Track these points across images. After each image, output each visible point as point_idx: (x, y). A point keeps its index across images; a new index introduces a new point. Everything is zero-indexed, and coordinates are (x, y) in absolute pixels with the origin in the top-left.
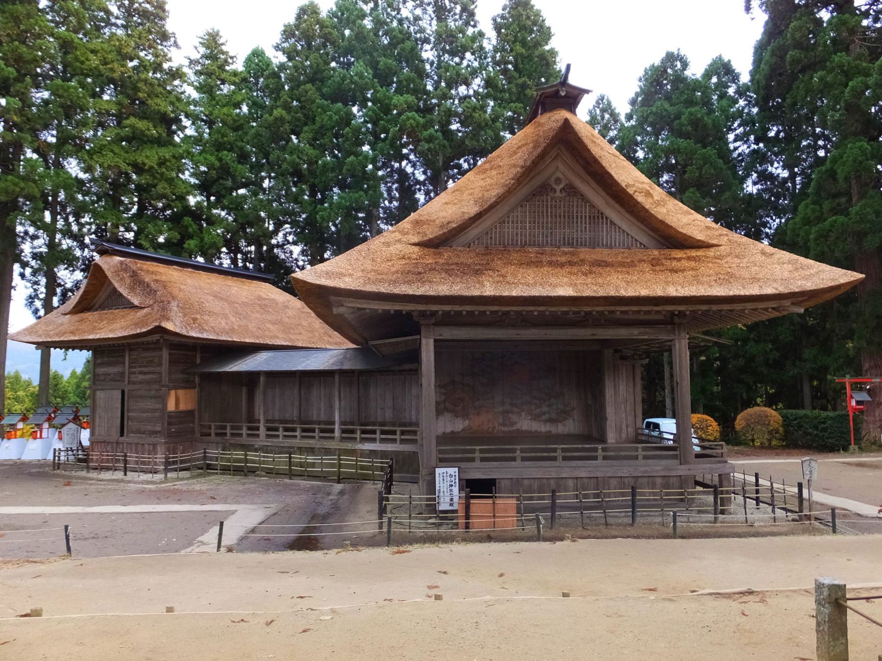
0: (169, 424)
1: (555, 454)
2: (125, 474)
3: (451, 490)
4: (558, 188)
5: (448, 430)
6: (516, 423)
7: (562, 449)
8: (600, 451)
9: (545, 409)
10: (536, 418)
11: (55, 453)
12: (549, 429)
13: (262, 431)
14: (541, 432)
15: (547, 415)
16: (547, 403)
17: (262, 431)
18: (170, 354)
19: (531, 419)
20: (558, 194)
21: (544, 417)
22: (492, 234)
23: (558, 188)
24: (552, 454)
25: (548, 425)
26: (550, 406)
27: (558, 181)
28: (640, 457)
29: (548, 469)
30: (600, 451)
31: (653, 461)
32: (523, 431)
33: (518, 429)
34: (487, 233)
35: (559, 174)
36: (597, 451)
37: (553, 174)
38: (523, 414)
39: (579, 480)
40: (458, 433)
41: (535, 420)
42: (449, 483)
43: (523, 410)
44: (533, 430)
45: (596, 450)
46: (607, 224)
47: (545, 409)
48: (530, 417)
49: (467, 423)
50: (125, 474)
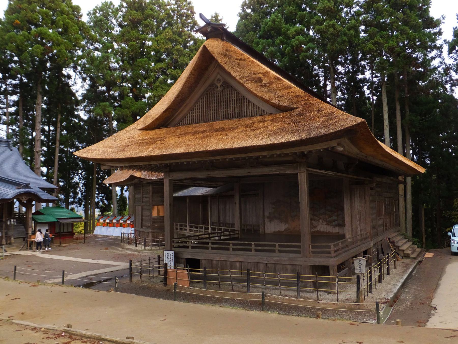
0: (154, 222)
1: (228, 247)
2: (136, 246)
3: (170, 263)
4: (219, 85)
5: (277, 230)
6: (316, 227)
7: (232, 243)
8: (253, 246)
9: (335, 218)
10: (329, 223)
11: (122, 235)
12: (337, 231)
13: (188, 228)
14: (332, 233)
15: (336, 222)
16: (336, 214)
17: (188, 228)
18: (153, 188)
19: (326, 224)
20: (219, 88)
21: (334, 223)
22: (187, 117)
23: (219, 85)
24: (227, 246)
25: (337, 228)
26: (338, 216)
27: (219, 80)
28: (277, 251)
29: (222, 255)
30: (253, 246)
31: (284, 254)
32: (321, 232)
33: (318, 231)
34: (185, 117)
35: (219, 77)
36: (252, 246)
37: (216, 77)
38: (321, 221)
39: (242, 263)
40: (282, 232)
41: (328, 225)
42: (170, 259)
43: (321, 218)
44: (327, 231)
45: (251, 245)
46: (247, 102)
47: (335, 218)
48: (325, 223)
49: (287, 226)
50: (136, 246)
